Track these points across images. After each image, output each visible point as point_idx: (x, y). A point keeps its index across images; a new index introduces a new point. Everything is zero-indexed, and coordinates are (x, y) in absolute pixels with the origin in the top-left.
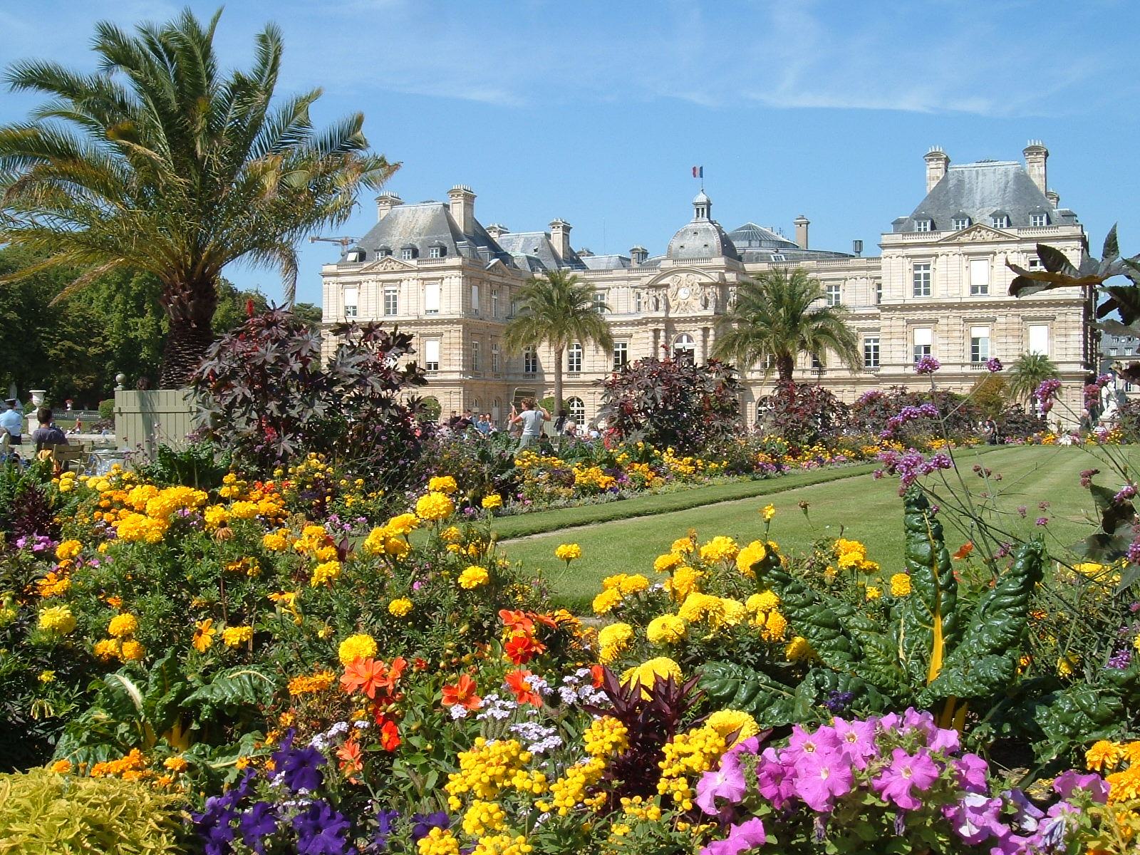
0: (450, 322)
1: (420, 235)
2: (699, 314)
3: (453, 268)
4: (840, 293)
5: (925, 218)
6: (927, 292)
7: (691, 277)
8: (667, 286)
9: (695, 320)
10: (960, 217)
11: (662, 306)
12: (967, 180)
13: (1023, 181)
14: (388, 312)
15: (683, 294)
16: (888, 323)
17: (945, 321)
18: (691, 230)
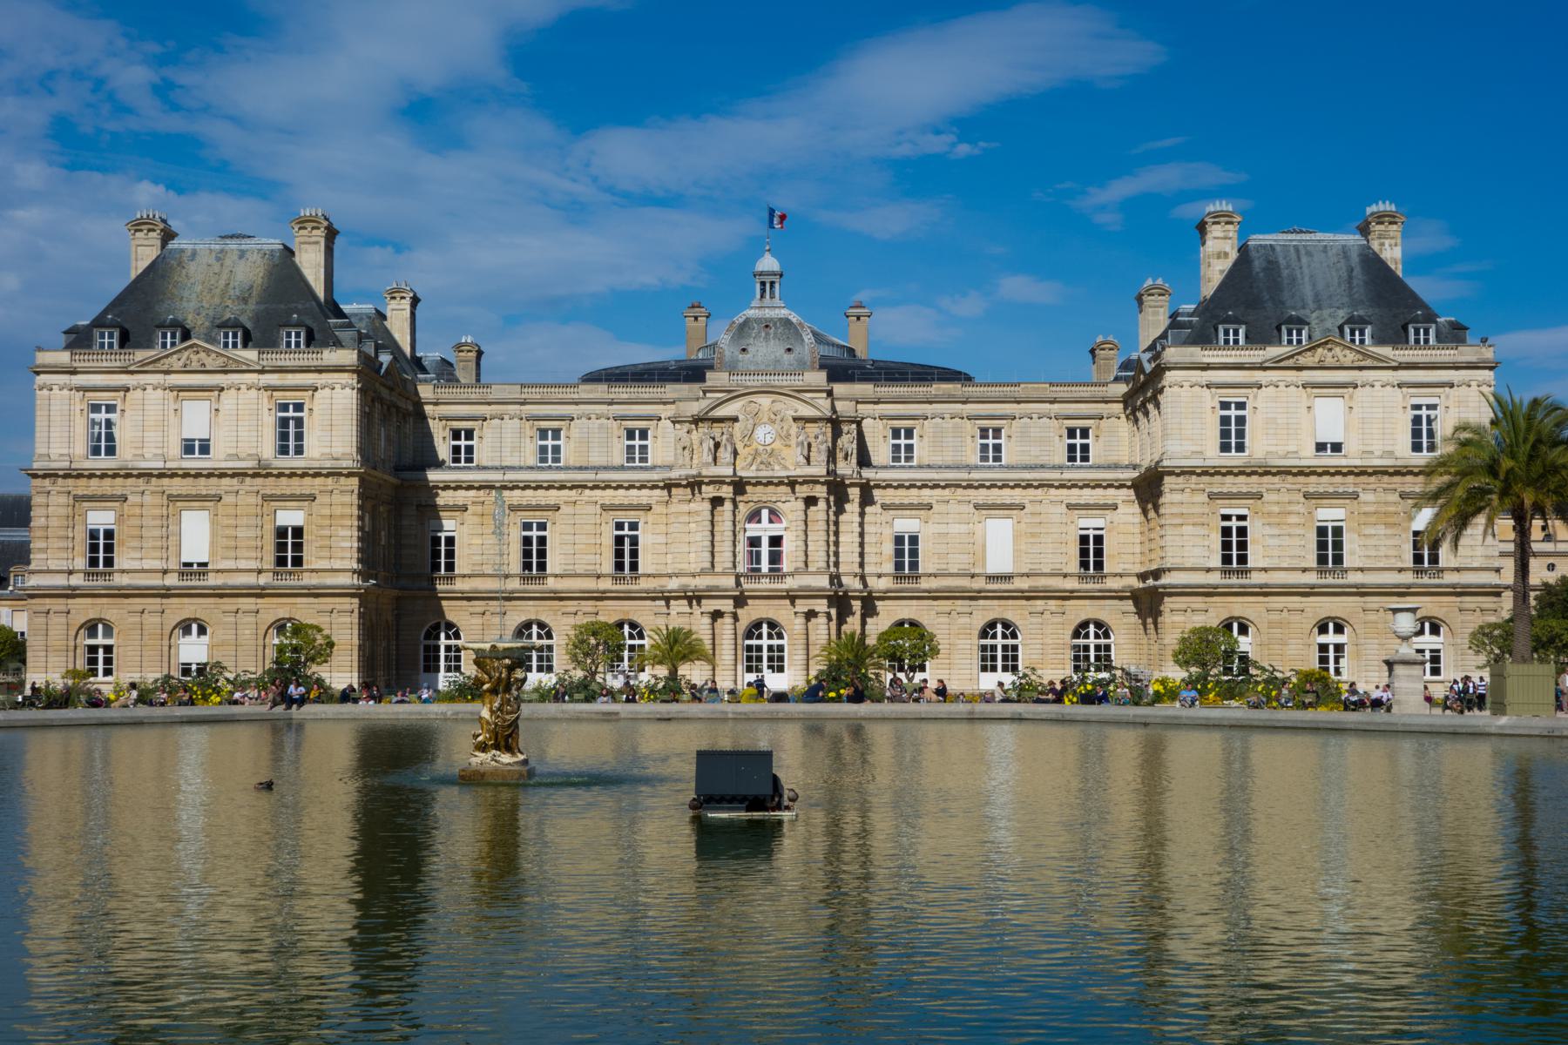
0: (334, 474)
1: (245, 300)
2: (799, 472)
4: (1002, 441)
5: (1237, 321)
6: (1240, 448)
7: (778, 406)
8: (735, 419)
9: (792, 483)
11: (725, 454)
12: (1282, 262)
13: (1373, 264)
15: (764, 434)
16: (1177, 497)
18: (758, 320)
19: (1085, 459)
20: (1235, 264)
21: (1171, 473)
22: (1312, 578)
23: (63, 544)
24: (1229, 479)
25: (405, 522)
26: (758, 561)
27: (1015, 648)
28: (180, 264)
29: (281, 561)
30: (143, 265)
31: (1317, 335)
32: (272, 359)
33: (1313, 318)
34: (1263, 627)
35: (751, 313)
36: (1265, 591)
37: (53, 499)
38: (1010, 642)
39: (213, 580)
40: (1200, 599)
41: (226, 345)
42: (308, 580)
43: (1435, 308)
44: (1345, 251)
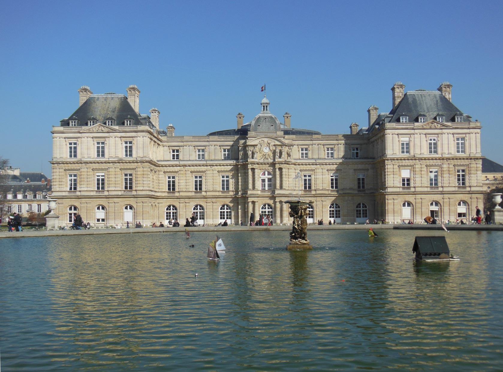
1: (114, 112)
3: (143, 131)
5: (406, 115)
10: (421, 115)
11: (255, 156)
12: (417, 99)
14: (98, 155)
15: (266, 150)
16: (389, 167)
17: (417, 166)
18: (263, 117)
19: (357, 156)
20: (403, 99)
21: (388, 160)
22: (429, 189)
23: (61, 183)
24: (404, 161)
25: (160, 176)
26: (265, 187)
27: (339, 211)
28: (94, 101)
29: (126, 188)
30: (84, 101)
31: (429, 119)
32: (122, 128)
33: (427, 115)
34: (414, 204)
35: (261, 115)
36: (414, 193)
37: (58, 170)
38: (338, 209)
39: (106, 193)
40: (396, 196)
41: (109, 125)
42: (134, 193)
43: (462, 112)
44: (435, 96)
